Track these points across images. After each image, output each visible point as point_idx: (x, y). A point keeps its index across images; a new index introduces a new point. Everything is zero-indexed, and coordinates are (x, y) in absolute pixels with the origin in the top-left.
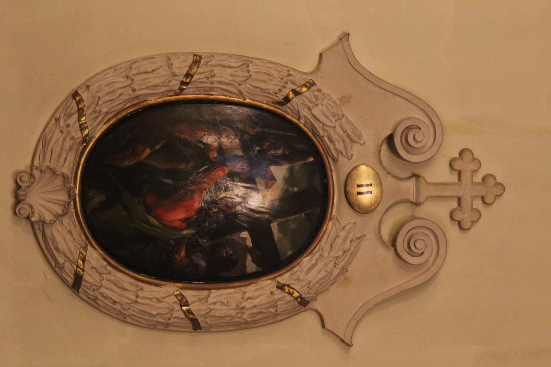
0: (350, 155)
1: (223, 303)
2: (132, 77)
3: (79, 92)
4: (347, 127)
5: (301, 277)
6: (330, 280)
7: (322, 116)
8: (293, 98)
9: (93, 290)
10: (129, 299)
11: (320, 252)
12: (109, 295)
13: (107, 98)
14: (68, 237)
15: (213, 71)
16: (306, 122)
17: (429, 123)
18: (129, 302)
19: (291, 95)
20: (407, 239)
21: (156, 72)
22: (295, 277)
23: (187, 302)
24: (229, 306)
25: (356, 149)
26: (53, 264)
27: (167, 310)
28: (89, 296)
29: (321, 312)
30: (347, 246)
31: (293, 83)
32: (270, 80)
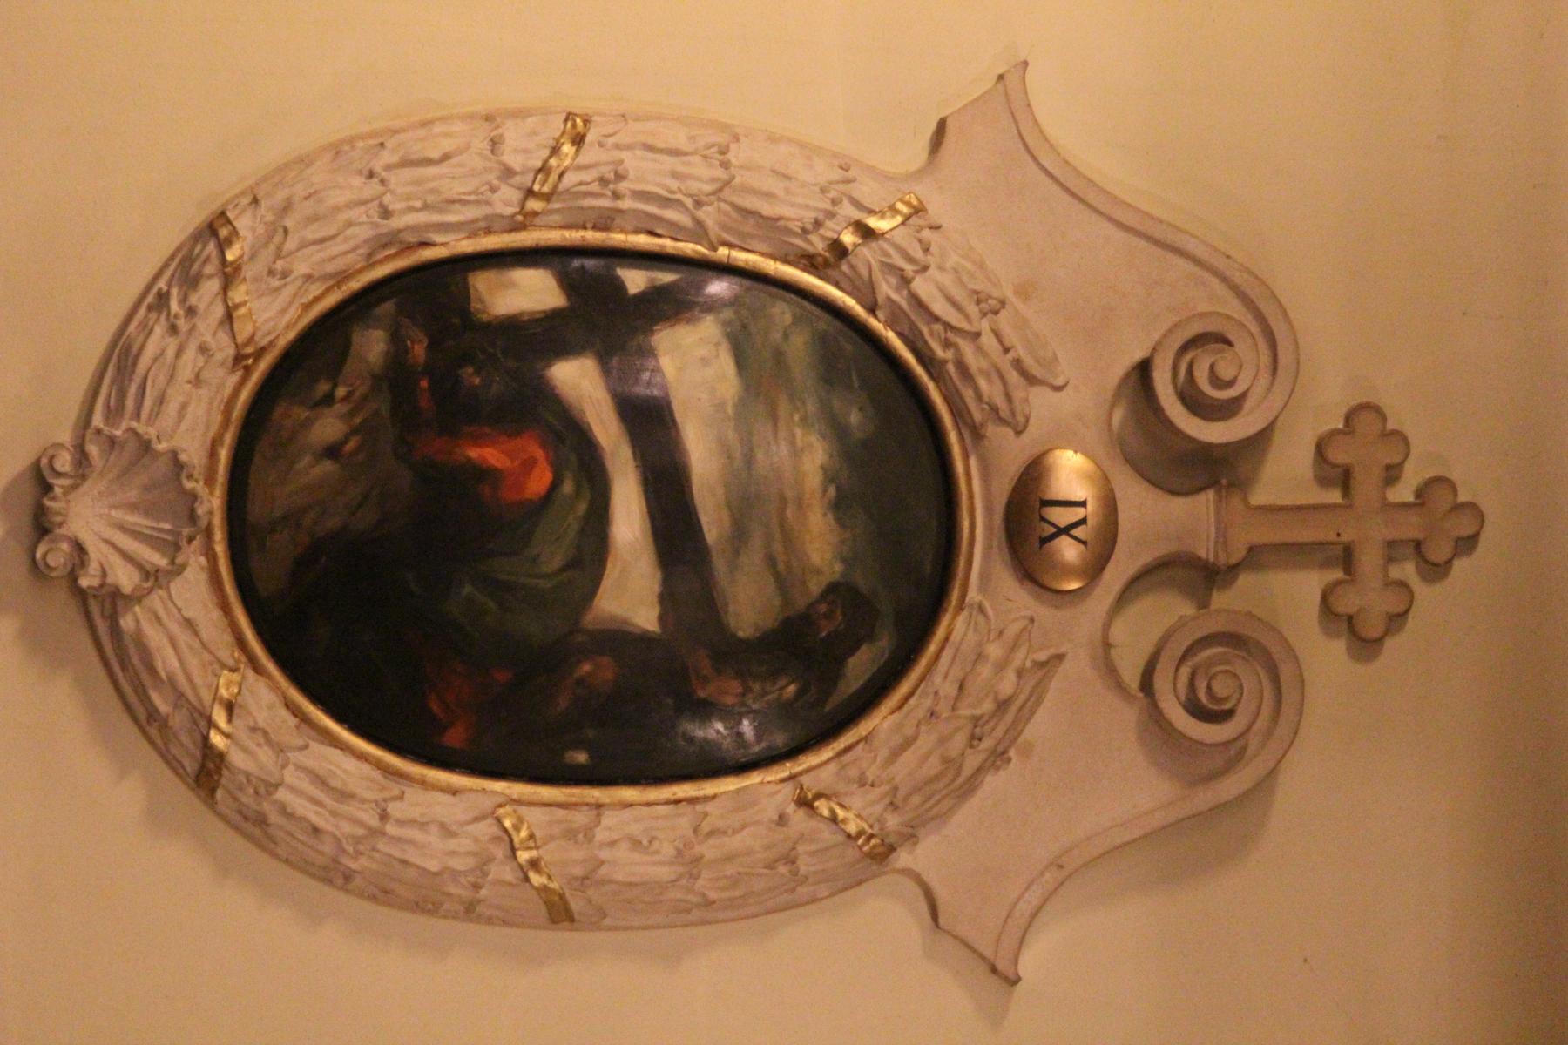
0: (1021, 419)
1: (636, 844)
2: (384, 174)
3: (230, 215)
4: (1011, 337)
8: (856, 246)
10: (361, 824)
12: (300, 811)
13: (312, 233)
14: (183, 637)
15: (621, 162)
17: (1254, 328)
18: (361, 832)
19: (848, 238)
21: (454, 161)
24: (657, 852)
25: (1040, 403)
26: (142, 716)
27: (470, 862)
30: (1007, 685)
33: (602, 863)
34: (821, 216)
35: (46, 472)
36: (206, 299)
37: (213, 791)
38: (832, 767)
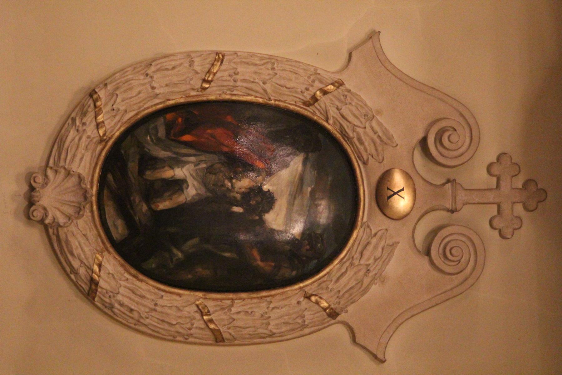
2: (151, 75)
3: (97, 90)
5: (330, 287)
6: (361, 289)
7: (350, 115)
9: (110, 297)
11: (350, 261)
14: (83, 241)
16: (334, 122)
18: (147, 310)
20: (442, 245)
21: (177, 69)
22: (324, 285)
23: (209, 311)
24: (253, 316)
26: (68, 270)
28: (105, 304)
29: (351, 324)
31: (321, 82)
32: (296, 78)
33: (234, 320)
34: (308, 86)
36: (90, 119)
37: (94, 299)
38: (316, 285)
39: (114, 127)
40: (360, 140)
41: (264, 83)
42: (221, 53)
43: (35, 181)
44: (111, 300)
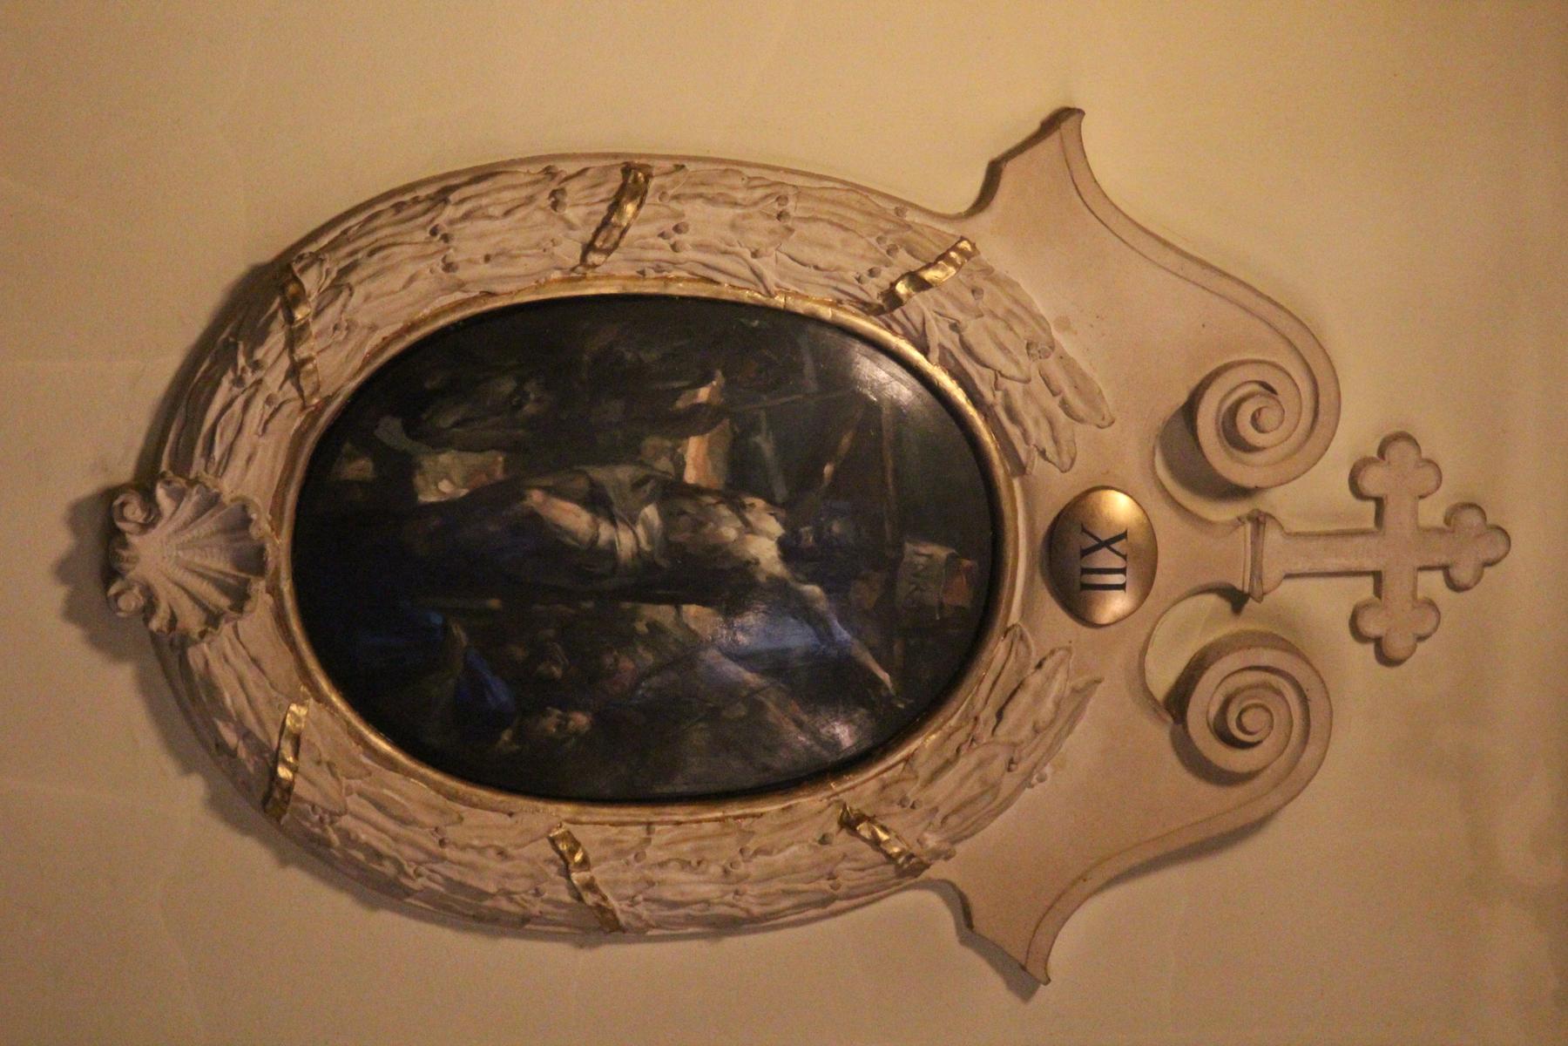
2: (447, 230)
3: (296, 267)
8: (909, 296)
14: (250, 675)
18: (421, 856)
19: (901, 288)
22: (894, 793)
24: (703, 873)
32: (845, 243)
35: (116, 514)
39: (338, 366)
40: (1010, 410)
41: (755, 255)
42: (641, 168)
43: (124, 519)
44: (325, 830)
